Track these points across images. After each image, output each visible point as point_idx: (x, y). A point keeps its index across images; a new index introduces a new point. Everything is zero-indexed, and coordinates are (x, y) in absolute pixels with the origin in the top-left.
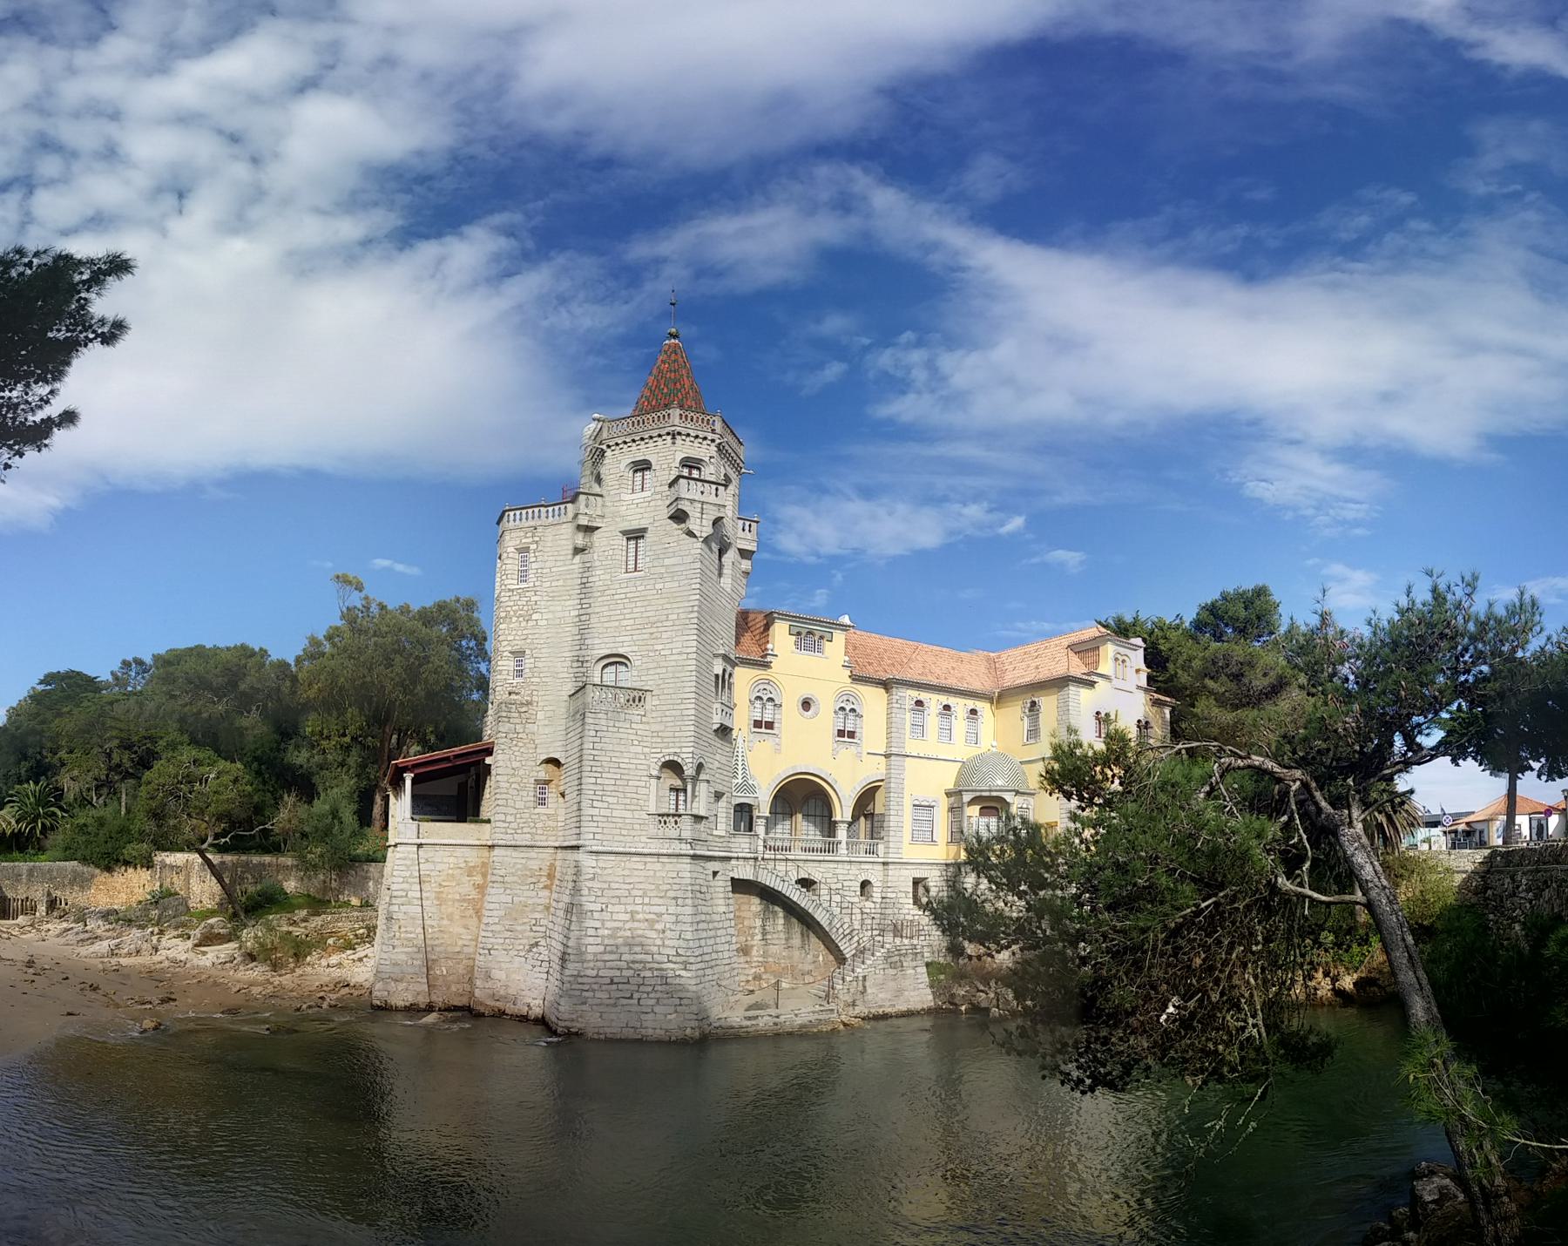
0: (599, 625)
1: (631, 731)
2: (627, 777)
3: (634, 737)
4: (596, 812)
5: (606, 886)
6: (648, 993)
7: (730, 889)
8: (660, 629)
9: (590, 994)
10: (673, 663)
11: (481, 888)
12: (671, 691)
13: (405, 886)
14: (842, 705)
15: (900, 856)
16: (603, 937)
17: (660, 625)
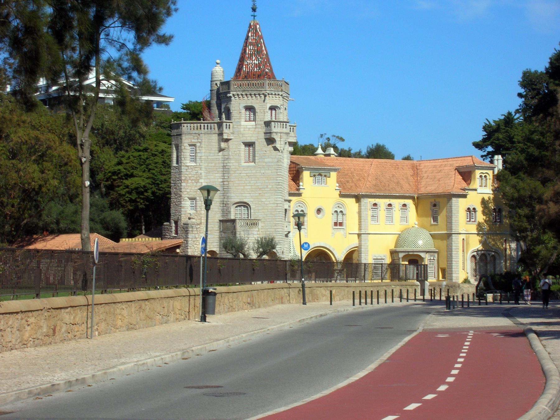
0: (234, 187)
10: (271, 208)
12: (270, 220)
14: (336, 209)
17: (264, 190)
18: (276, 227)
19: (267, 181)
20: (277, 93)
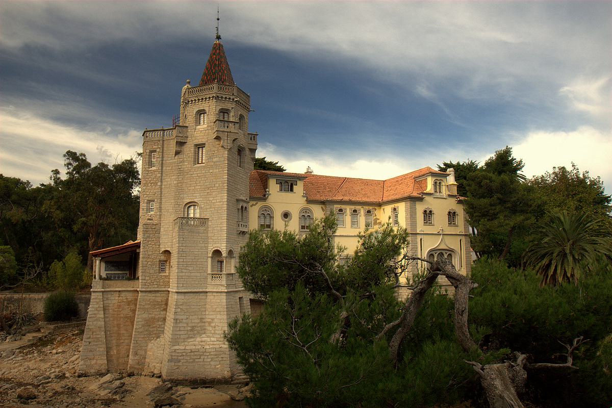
1: (199, 237)
4: (184, 274)
5: (188, 307)
6: (207, 356)
7: (249, 304)
9: (182, 358)
10: (217, 206)
11: (134, 311)
12: (216, 218)
13: (96, 312)
16: (187, 330)
19: (214, 180)
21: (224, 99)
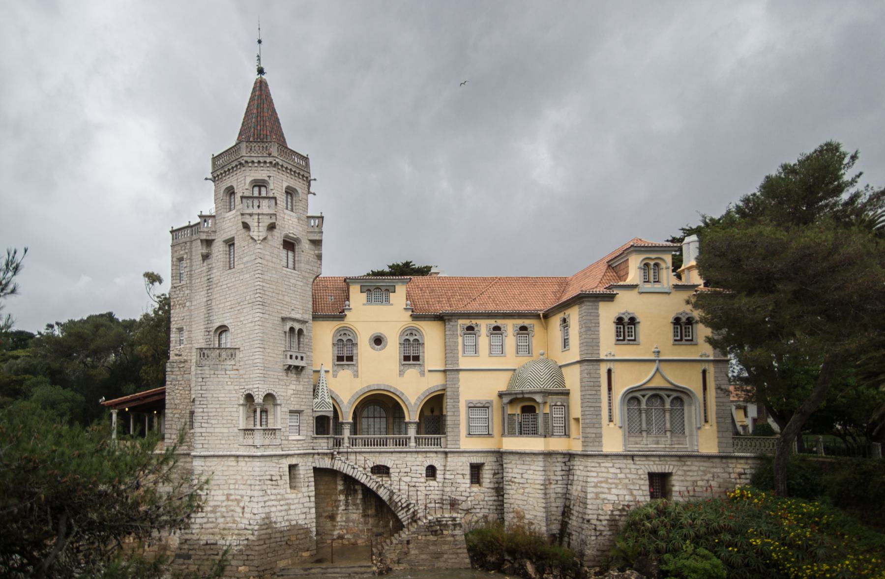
1: (225, 376)
2: (224, 406)
3: (227, 380)
4: (203, 430)
8: (243, 307)
15: (457, 446)
18: (253, 358)
20: (262, 160)
21: (256, 165)
